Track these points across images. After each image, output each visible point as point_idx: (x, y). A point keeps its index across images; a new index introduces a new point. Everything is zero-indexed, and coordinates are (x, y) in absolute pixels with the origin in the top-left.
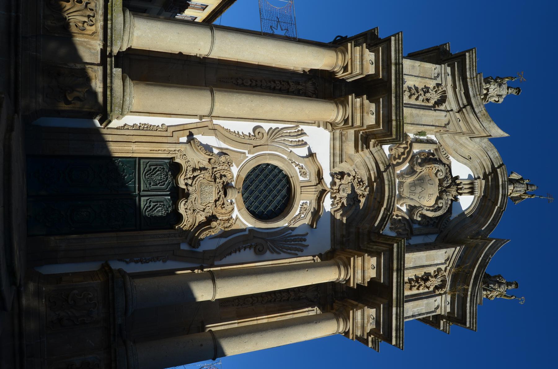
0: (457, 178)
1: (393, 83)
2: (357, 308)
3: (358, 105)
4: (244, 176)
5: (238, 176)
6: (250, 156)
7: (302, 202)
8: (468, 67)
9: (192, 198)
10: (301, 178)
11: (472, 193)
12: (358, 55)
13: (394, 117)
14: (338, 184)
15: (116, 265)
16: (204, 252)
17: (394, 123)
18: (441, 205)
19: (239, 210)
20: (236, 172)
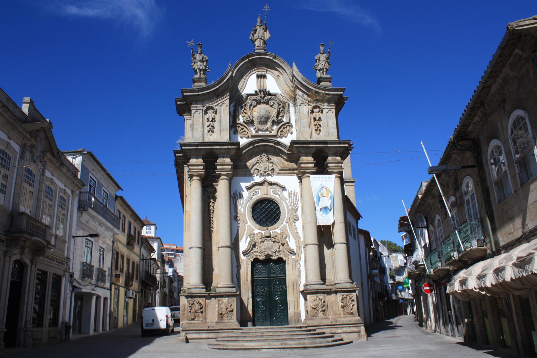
0: (256, 92)
1: (208, 147)
2: (327, 166)
3: (220, 167)
4: (258, 226)
5: (259, 229)
6: (249, 223)
7: (272, 194)
8: (192, 94)
9: (270, 253)
10: (259, 194)
11: (264, 77)
12: (194, 167)
13: (226, 147)
14: (261, 172)
15: (302, 288)
16: (296, 246)
17: (229, 147)
18: (272, 103)
19: (276, 229)
20: (257, 230)
